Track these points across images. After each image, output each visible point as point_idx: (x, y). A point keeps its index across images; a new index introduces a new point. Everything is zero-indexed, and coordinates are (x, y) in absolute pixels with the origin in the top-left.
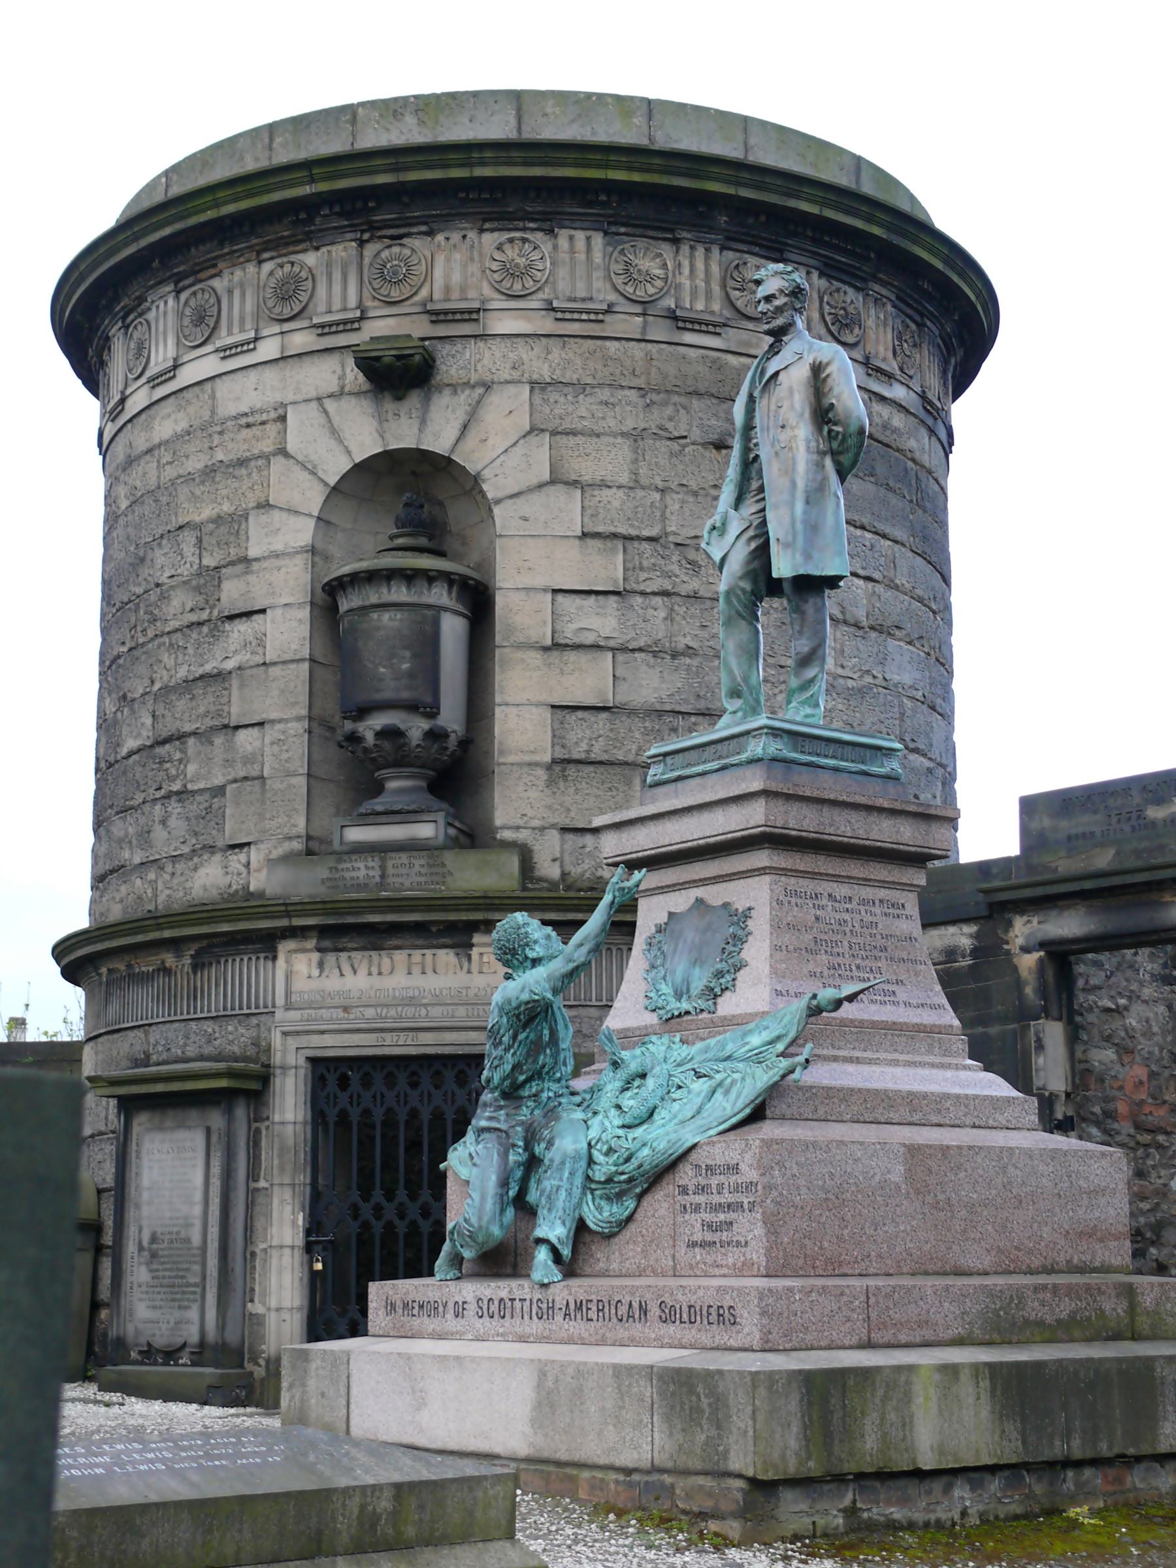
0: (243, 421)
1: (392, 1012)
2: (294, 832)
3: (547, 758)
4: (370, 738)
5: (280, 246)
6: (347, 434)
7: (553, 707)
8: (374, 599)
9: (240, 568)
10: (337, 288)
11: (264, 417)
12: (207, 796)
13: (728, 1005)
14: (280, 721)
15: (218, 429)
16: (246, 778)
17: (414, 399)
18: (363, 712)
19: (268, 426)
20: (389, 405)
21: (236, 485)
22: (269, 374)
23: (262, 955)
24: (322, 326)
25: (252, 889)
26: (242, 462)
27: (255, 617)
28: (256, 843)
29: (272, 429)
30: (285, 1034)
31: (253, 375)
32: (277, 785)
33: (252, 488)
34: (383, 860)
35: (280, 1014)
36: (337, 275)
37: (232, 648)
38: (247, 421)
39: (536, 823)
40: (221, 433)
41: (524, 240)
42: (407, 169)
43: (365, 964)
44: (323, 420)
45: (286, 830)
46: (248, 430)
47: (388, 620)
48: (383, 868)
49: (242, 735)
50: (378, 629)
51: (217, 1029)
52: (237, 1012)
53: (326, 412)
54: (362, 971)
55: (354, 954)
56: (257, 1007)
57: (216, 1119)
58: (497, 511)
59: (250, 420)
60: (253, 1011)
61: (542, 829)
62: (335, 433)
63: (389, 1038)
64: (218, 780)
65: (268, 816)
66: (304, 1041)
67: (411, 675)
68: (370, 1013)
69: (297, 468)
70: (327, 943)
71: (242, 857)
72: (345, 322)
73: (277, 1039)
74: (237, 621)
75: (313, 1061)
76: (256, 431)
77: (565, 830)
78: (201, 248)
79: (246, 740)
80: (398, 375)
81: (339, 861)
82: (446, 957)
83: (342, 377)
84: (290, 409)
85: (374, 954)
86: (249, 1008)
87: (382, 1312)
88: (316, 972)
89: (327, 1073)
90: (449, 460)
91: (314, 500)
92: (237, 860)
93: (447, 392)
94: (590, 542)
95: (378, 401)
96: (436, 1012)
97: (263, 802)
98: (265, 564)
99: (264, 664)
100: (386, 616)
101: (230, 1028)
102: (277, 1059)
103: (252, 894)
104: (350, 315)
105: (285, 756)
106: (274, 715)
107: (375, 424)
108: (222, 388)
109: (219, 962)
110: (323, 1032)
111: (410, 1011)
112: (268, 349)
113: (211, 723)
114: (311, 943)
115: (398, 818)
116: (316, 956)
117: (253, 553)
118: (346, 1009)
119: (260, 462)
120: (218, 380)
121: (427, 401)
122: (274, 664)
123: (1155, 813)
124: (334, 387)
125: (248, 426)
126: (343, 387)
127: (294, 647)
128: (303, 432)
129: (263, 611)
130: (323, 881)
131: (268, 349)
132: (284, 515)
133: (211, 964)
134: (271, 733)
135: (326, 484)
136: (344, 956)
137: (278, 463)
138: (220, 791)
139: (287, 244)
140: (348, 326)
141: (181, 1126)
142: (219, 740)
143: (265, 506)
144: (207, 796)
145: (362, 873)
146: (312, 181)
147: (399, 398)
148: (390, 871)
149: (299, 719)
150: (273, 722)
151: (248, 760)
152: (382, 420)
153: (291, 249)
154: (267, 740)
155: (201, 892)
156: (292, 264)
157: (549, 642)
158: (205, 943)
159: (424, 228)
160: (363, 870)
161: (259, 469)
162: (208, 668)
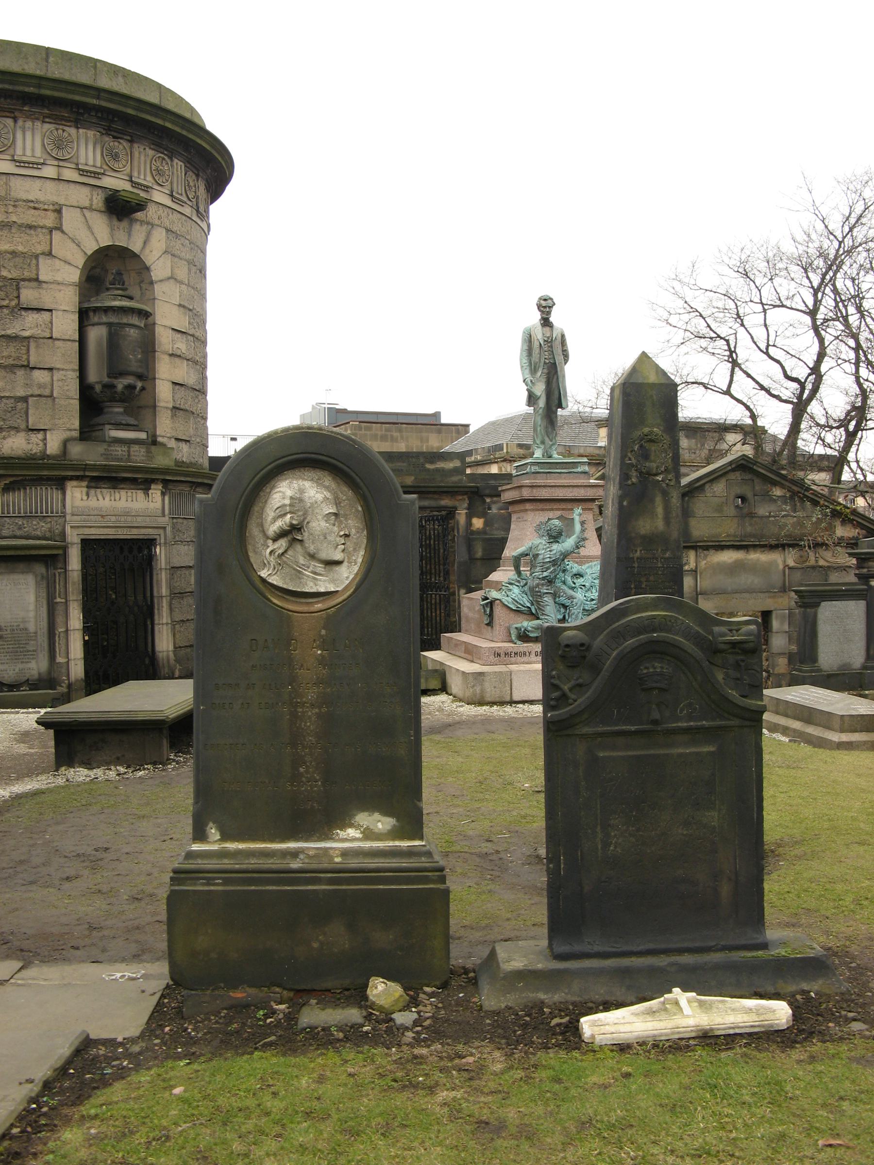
0: (32, 205)
1: (123, 519)
2: (73, 427)
3: (171, 406)
4: (120, 387)
5: (57, 119)
6: (95, 231)
7: (173, 383)
8: (125, 321)
9: (35, 284)
10: (91, 154)
11: (46, 207)
12: (12, 401)
13: (583, 552)
14: (63, 370)
15: (12, 203)
16: (40, 396)
17: (125, 223)
18: (122, 374)
19: (49, 213)
20: (115, 222)
21: (28, 238)
22: (50, 185)
23: (54, 487)
24: (83, 171)
25: (48, 452)
26: (30, 227)
27: (43, 312)
28: (50, 430)
29: (52, 216)
30: (71, 527)
31: (38, 182)
32: (62, 402)
33: (39, 243)
34: (129, 447)
35: (68, 517)
36: (91, 147)
37: (28, 325)
38: (34, 205)
39: (168, 435)
40: (14, 206)
41: (163, 159)
42: (142, 111)
43: (108, 494)
44: (83, 220)
45: (68, 426)
46: (34, 211)
47: (133, 332)
48: (129, 451)
49: (36, 373)
50: (130, 336)
51: (25, 522)
52: (39, 514)
53: (84, 215)
54: (107, 498)
55: (103, 490)
56: (52, 513)
57: (41, 569)
58: (156, 286)
59: (36, 205)
60: (49, 514)
61: (170, 438)
62: (89, 228)
63: (120, 531)
64: (21, 392)
65: (57, 417)
66: (81, 531)
67: (140, 361)
68: (113, 519)
69: (69, 241)
70: (93, 484)
71: (40, 436)
72: (95, 173)
73: (68, 530)
74: (30, 312)
75: (82, 540)
76: (42, 213)
77: (177, 439)
78: (9, 101)
79: (40, 376)
80: (121, 208)
81: (109, 446)
82: (140, 494)
83: (91, 200)
84: (64, 208)
85: (112, 491)
86: (47, 513)
87: (492, 657)
88: (85, 498)
89: (87, 544)
90: (135, 256)
91: (80, 261)
92: (37, 438)
93: (138, 223)
94: (182, 309)
95: (110, 219)
96: (139, 519)
97: (54, 410)
98: (51, 286)
99: (51, 338)
100: (132, 331)
101: (34, 523)
102: (69, 539)
103: (48, 456)
104: (99, 170)
105: (66, 388)
106: (58, 366)
107: (109, 230)
108: (15, 182)
109: (25, 489)
110: (90, 527)
111: (129, 519)
112: (49, 171)
113: (12, 362)
114: (85, 484)
115: (132, 428)
116: (85, 490)
117: (41, 278)
118: (102, 516)
119: (44, 231)
120: (12, 177)
121: (131, 225)
122: (59, 340)
123: (429, 466)
124: (87, 204)
125: (35, 208)
126: (91, 205)
127: (69, 333)
128: (71, 220)
129: (50, 311)
130: (102, 455)
131: (49, 171)
132: (62, 263)
133: (19, 489)
134: (57, 375)
135: (85, 253)
136: (99, 490)
137: (56, 235)
138: (25, 399)
139: (62, 120)
140: (96, 175)
141: (13, 572)
142: (20, 373)
143: (50, 254)
144: (12, 401)
145: (120, 452)
146: (98, 98)
147: (120, 220)
148: (132, 453)
149: (74, 370)
150: (58, 369)
151: (40, 386)
152: (112, 229)
153: (63, 123)
154: (55, 378)
155: (9, 451)
156: (64, 131)
157: (171, 352)
158: (12, 479)
159: (129, 138)
160: (120, 450)
161: (43, 234)
162: (9, 332)
